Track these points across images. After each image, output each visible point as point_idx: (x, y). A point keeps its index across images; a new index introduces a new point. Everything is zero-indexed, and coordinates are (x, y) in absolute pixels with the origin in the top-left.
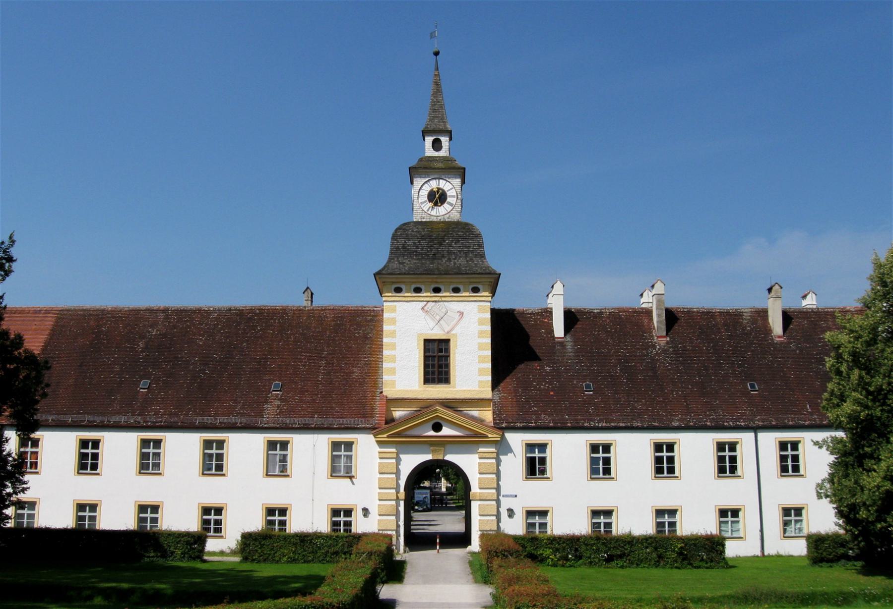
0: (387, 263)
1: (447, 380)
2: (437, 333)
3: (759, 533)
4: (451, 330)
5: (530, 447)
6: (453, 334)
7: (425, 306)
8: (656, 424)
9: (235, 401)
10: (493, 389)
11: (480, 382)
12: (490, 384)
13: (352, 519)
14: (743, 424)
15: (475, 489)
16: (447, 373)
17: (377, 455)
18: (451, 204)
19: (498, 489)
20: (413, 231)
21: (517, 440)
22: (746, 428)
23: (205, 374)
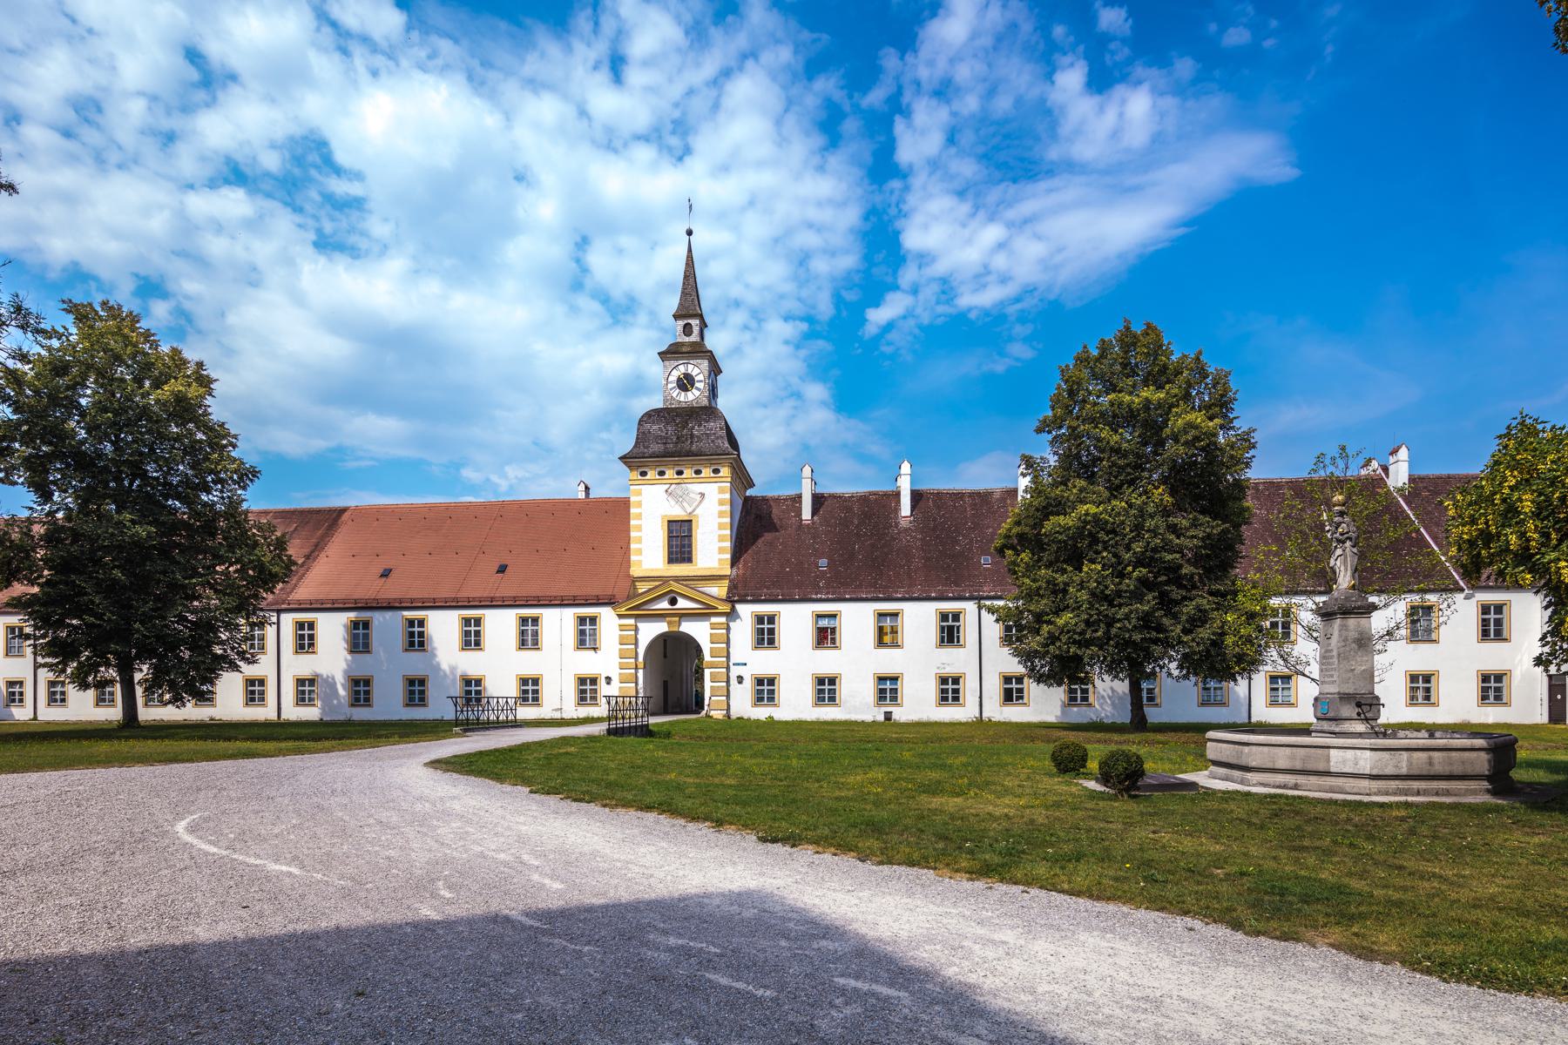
1: (690, 560)
3: (978, 700)
4: (694, 511)
5: (760, 619)
10: (732, 567)
11: (720, 560)
12: (729, 562)
13: (598, 687)
15: (707, 657)
16: (690, 552)
17: (618, 628)
18: (698, 389)
19: (728, 657)
21: (746, 611)
22: (970, 598)
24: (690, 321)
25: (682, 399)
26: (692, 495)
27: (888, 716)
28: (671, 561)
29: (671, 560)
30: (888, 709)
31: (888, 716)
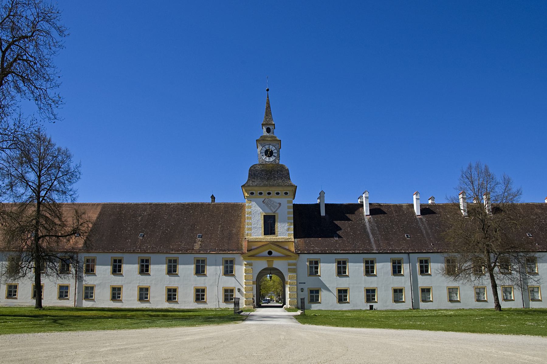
0: (247, 181)
1: (274, 233)
2: (270, 213)
6: (276, 213)
7: (264, 200)
8: (366, 252)
9: (181, 242)
14: (403, 252)
20: (258, 167)
23: (168, 231)
24: (269, 127)
25: (267, 160)
26: (275, 204)
27: (371, 307)
28: (265, 234)
29: (265, 234)
30: (371, 304)
31: (371, 307)
